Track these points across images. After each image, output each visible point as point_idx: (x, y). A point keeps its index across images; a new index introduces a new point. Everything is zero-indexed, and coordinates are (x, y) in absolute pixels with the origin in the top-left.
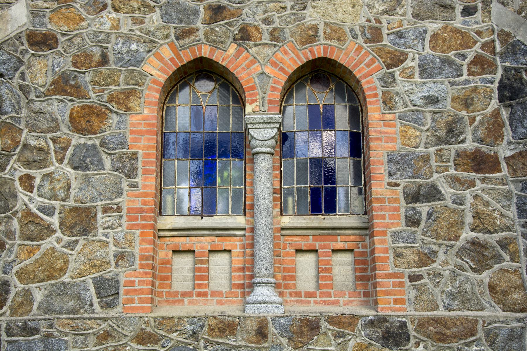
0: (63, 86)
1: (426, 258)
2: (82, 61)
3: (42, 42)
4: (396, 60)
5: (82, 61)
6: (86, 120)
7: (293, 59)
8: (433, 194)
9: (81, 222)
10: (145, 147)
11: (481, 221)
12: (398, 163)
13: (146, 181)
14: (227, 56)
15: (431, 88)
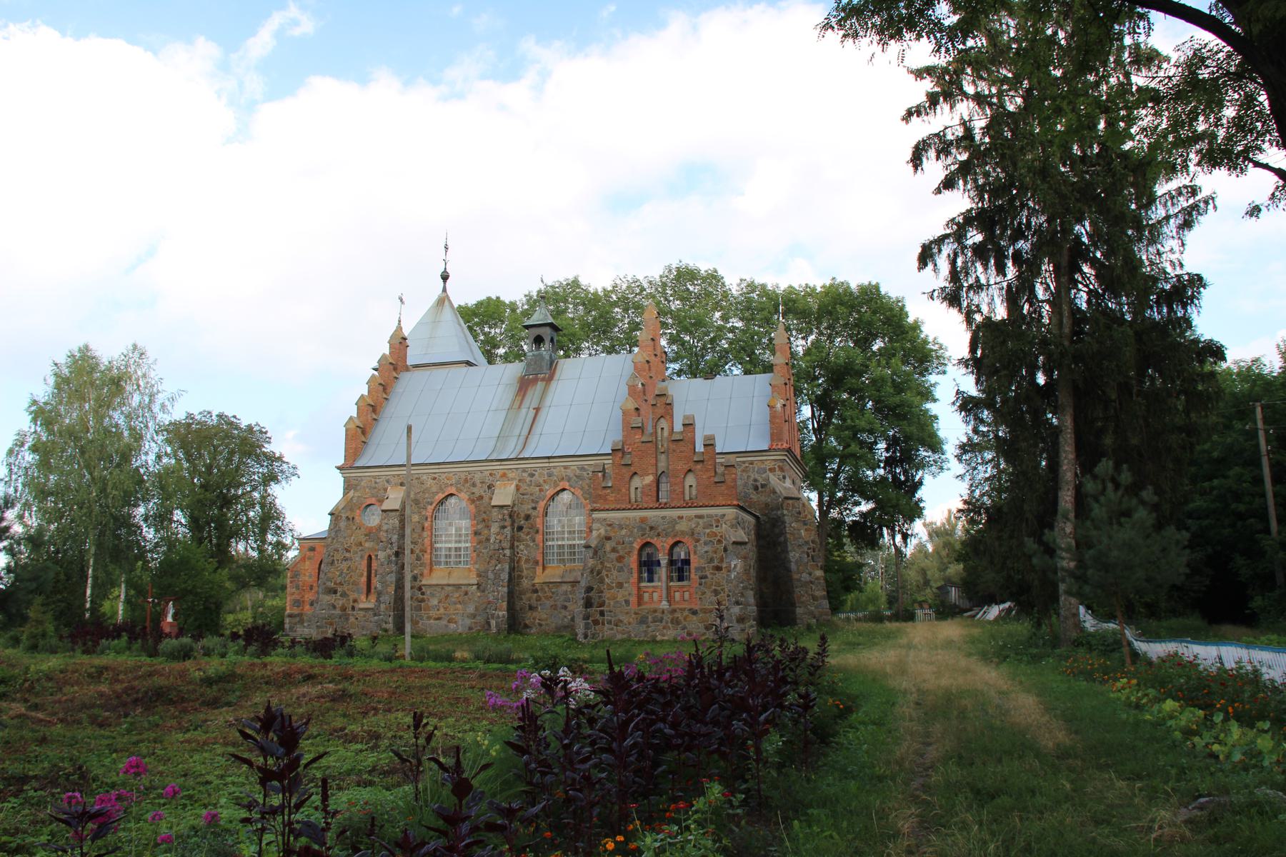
0: (614, 550)
1: (704, 593)
2: (618, 543)
3: (608, 538)
4: (698, 541)
5: (618, 543)
6: (620, 559)
7: (671, 541)
8: (706, 577)
9: (620, 585)
10: (634, 566)
11: (718, 584)
12: (697, 569)
13: (635, 575)
14: (654, 541)
15: (706, 549)
